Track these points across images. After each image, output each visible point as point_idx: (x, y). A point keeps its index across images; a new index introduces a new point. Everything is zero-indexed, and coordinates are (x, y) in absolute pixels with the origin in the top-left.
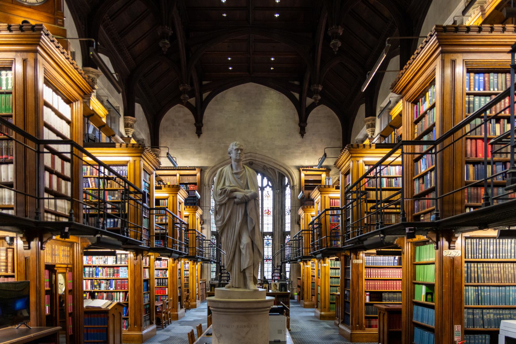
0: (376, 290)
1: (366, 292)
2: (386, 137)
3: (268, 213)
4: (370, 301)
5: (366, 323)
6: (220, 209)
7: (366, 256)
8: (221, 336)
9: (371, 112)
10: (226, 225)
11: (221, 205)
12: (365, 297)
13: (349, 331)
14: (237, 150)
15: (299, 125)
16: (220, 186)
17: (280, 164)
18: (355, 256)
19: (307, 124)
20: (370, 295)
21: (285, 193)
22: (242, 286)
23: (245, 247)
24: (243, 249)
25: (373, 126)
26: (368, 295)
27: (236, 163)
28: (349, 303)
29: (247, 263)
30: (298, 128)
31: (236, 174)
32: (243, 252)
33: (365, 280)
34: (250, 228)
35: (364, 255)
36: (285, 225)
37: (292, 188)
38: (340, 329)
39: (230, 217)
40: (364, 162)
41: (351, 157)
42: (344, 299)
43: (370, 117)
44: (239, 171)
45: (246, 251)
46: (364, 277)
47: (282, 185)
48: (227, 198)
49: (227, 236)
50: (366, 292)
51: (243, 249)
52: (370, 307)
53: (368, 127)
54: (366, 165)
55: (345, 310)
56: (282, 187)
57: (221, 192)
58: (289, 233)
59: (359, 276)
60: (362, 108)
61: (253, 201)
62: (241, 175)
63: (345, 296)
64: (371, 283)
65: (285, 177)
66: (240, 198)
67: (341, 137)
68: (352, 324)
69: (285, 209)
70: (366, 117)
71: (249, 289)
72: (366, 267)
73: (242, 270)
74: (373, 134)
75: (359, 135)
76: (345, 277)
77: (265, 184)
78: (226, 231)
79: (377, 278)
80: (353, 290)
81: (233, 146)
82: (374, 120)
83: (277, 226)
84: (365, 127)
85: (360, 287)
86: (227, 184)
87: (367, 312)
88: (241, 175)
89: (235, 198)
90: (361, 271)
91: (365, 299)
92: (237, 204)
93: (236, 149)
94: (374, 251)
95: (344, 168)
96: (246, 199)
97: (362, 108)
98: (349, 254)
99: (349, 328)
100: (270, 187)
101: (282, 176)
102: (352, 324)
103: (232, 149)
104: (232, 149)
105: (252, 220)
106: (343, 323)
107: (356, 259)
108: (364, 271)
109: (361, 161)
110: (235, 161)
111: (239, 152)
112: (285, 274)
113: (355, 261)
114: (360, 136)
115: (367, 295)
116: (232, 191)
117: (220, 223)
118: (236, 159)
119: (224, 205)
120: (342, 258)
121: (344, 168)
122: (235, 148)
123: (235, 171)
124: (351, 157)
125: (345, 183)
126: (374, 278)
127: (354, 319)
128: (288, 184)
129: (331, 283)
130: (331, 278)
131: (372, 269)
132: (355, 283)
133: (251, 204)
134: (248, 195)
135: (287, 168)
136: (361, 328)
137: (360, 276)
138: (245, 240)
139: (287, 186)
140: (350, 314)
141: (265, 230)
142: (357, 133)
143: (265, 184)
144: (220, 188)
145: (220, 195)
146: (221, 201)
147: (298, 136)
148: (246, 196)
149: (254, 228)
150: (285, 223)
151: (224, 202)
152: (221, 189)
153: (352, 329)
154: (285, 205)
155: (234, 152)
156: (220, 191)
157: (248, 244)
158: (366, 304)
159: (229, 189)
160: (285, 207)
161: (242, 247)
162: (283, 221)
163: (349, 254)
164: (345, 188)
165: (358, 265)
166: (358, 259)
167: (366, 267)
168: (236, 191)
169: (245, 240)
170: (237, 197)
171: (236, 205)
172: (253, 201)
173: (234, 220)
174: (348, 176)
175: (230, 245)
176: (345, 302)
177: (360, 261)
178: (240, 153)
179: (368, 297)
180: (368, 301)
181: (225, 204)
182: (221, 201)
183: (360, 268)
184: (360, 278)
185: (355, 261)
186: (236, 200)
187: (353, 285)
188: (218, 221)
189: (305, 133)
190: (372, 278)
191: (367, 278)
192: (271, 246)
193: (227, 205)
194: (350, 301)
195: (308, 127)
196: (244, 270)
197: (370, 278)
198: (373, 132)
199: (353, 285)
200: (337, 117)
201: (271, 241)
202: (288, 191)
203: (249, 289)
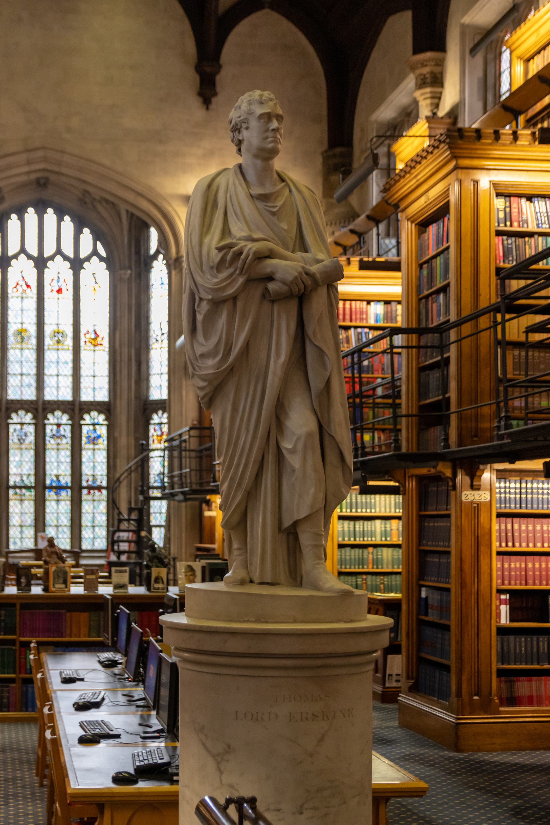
0: (530, 587)
1: (500, 592)
2: (520, 113)
3: (95, 341)
4: (511, 621)
5: (499, 688)
6: (210, 318)
7: (499, 479)
8: (229, 749)
9: (430, 37)
10: (231, 370)
11: (216, 304)
12: (498, 608)
13: (450, 718)
14: (268, 117)
15: (199, 68)
16: (213, 239)
17: (139, 188)
18: (467, 480)
19: (220, 67)
20: (511, 603)
21: (148, 280)
22: (283, 578)
23: (300, 446)
24: (293, 451)
25: (436, 81)
26: (505, 602)
27: (259, 162)
28: (447, 628)
29: (308, 500)
30: (193, 78)
31: (264, 198)
32: (294, 461)
33: (499, 553)
34: (316, 383)
35: (494, 477)
36: (148, 380)
37: (173, 265)
38: (404, 709)
39: (247, 346)
40: (495, 185)
41: (456, 168)
42: (418, 613)
43: (428, 55)
44: (268, 190)
45: (304, 460)
46: (495, 545)
47: (138, 252)
48: (241, 280)
49: (235, 409)
50: (500, 592)
51: (293, 451)
52: (512, 638)
53: (422, 83)
54: (498, 195)
55: (419, 650)
56: (138, 262)
57: (222, 260)
58: (161, 405)
59: (480, 540)
60: (400, 27)
61: (323, 291)
62: (279, 203)
63: (423, 606)
64: (516, 564)
65: (147, 227)
66: (290, 278)
67: (324, 111)
68: (459, 694)
69: (147, 330)
70: (416, 51)
71: (316, 588)
72: (499, 515)
73: (287, 523)
74: (437, 106)
75: (382, 108)
76: (420, 543)
77: (86, 249)
78: (230, 390)
79: (531, 549)
80: (462, 585)
81: (250, 103)
82: (441, 63)
83: (125, 384)
84: (410, 81)
85: (484, 577)
86: (238, 230)
87: (503, 658)
88: (279, 203)
89: (270, 278)
90: (487, 526)
91: (499, 615)
92: (273, 302)
93: (261, 116)
94: (538, 464)
95: (422, 202)
96: (309, 282)
97: (400, 27)
98: (448, 473)
99: (448, 709)
100: (101, 259)
101: (139, 226)
102: (459, 694)
103: (250, 113)
104: (250, 113)
105: (321, 353)
106: (415, 689)
107: (473, 487)
108: (495, 527)
109: (485, 180)
110: (256, 156)
111: (275, 124)
112: (150, 532)
113: (468, 496)
114: (387, 113)
115: (501, 602)
116: (262, 257)
117: (211, 362)
118: (262, 150)
119: (229, 305)
120: (411, 485)
121: (422, 202)
122: (259, 110)
123: (257, 191)
124: (456, 168)
125: (421, 248)
126: (524, 549)
127: (464, 677)
128: (158, 252)
129: (341, 562)
130: (341, 546)
131: (516, 520)
132: (467, 567)
133: (318, 303)
134: (314, 268)
135: (159, 202)
136: (486, 707)
137: (483, 541)
138: (300, 421)
139: (155, 257)
140: (453, 663)
141: (13, 394)
142: (381, 99)
143: (86, 249)
144: (214, 244)
145: (220, 266)
146: (224, 289)
147: (195, 102)
148: (307, 274)
149: (328, 383)
150: (148, 375)
151: (230, 291)
152: (220, 249)
153: (459, 711)
154: (147, 318)
155: (254, 124)
156: (216, 257)
157: (309, 435)
158: (502, 631)
159: (250, 247)
160: (148, 323)
161: (286, 445)
162: (143, 368)
163: (448, 473)
164: (421, 266)
165: (476, 508)
166: (478, 489)
167: (499, 515)
168: (271, 255)
169: (300, 421)
170: (278, 276)
171: (267, 306)
172: (323, 291)
173: (263, 355)
174: (432, 229)
175: (245, 439)
176: (421, 624)
177: (483, 496)
178: (275, 130)
179: (504, 609)
180: (504, 620)
181: (234, 298)
182: (224, 289)
183: (483, 518)
184: (483, 549)
185: (468, 496)
186: (272, 286)
187: (461, 569)
188: (202, 356)
189: (215, 94)
190: (517, 549)
191: (504, 549)
192: (103, 443)
193: (239, 304)
194: (453, 623)
195: (224, 78)
196: (296, 524)
197: (510, 549)
198: (437, 98)
199: (461, 569)
200: (310, 50)
201: (103, 431)
202: (159, 273)
203: (316, 588)
